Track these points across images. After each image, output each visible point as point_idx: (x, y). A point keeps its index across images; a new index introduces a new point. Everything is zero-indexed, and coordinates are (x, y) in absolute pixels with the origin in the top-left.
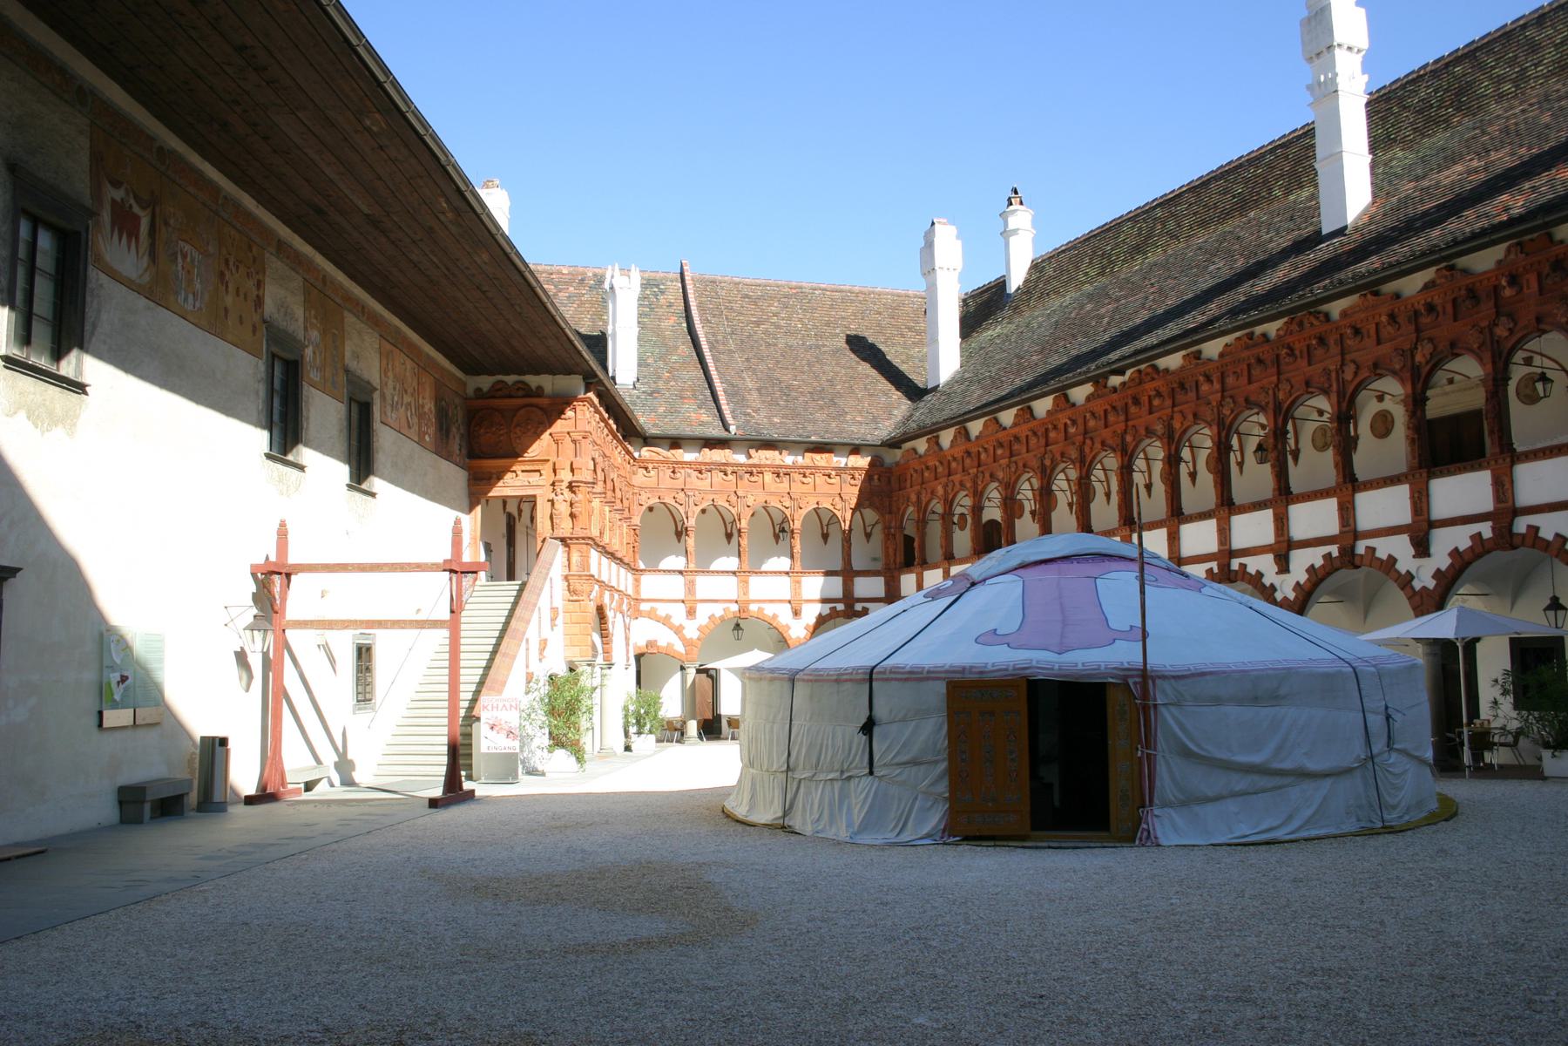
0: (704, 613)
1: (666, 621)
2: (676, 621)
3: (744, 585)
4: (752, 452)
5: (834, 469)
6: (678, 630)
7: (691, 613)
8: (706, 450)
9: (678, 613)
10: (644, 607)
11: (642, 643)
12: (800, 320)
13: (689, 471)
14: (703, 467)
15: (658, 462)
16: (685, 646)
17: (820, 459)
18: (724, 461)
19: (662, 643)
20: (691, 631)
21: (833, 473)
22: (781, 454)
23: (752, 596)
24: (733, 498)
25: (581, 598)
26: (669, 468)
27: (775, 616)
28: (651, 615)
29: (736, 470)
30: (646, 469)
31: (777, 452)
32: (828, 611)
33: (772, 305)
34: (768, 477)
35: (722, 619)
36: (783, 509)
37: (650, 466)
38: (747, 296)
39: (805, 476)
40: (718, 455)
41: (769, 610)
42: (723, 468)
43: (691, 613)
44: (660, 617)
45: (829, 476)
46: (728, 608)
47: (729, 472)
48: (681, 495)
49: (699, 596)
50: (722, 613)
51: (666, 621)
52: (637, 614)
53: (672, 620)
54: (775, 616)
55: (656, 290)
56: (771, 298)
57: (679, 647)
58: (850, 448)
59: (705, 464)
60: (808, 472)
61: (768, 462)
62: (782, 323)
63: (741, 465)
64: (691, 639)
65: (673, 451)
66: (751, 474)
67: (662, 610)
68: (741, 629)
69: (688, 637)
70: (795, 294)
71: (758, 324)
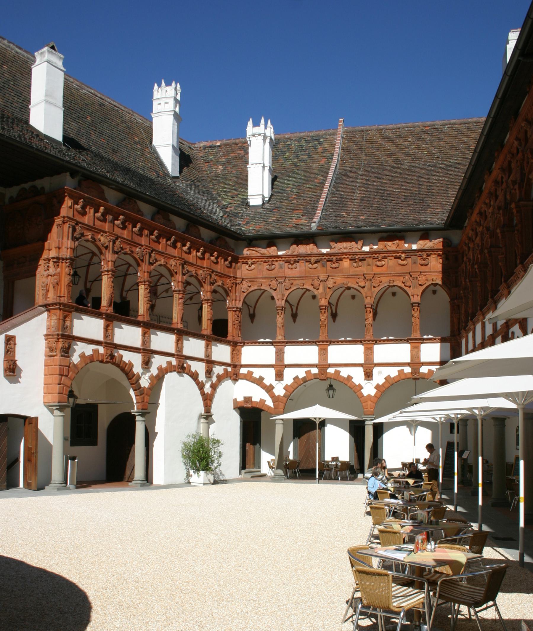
0: (289, 375)
1: (259, 382)
2: (267, 382)
3: (323, 353)
4: (333, 244)
5: (404, 252)
6: (269, 389)
7: (279, 376)
8: (294, 246)
9: (269, 376)
10: (243, 371)
11: (240, 399)
12: (427, 148)
13: (281, 263)
14: (292, 259)
15: (256, 257)
16: (273, 402)
17: (391, 246)
18: (309, 252)
19: (256, 399)
20: (279, 390)
21: (403, 255)
22: (357, 243)
23: (330, 361)
24: (316, 282)
25: (55, 354)
26: (265, 262)
27: (350, 378)
28: (249, 377)
29: (319, 259)
30: (247, 263)
31: (354, 243)
32: (397, 374)
33: (406, 141)
34: (346, 263)
35: (305, 380)
36: (359, 288)
37: (250, 261)
38: (387, 137)
39: (379, 261)
40: (303, 249)
41: (345, 372)
42: (307, 258)
43: (279, 376)
44: (256, 379)
45: (399, 258)
46: (310, 371)
47: (312, 261)
48: (274, 282)
49: (286, 362)
50: (304, 375)
51: (259, 382)
52: (235, 377)
53: (264, 381)
54: (350, 378)
55: (316, 142)
56: (407, 136)
57: (269, 402)
58: (420, 233)
59: (293, 256)
60: (380, 256)
61: (345, 251)
62: (411, 152)
63: (323, 255)
64: (279, 396)
65: (268, 249)
66: (331, 261)
67: (257, 373)
68: (334, 390)
69: (277, 394)
70: (428, 131)
71: (390, 156)
